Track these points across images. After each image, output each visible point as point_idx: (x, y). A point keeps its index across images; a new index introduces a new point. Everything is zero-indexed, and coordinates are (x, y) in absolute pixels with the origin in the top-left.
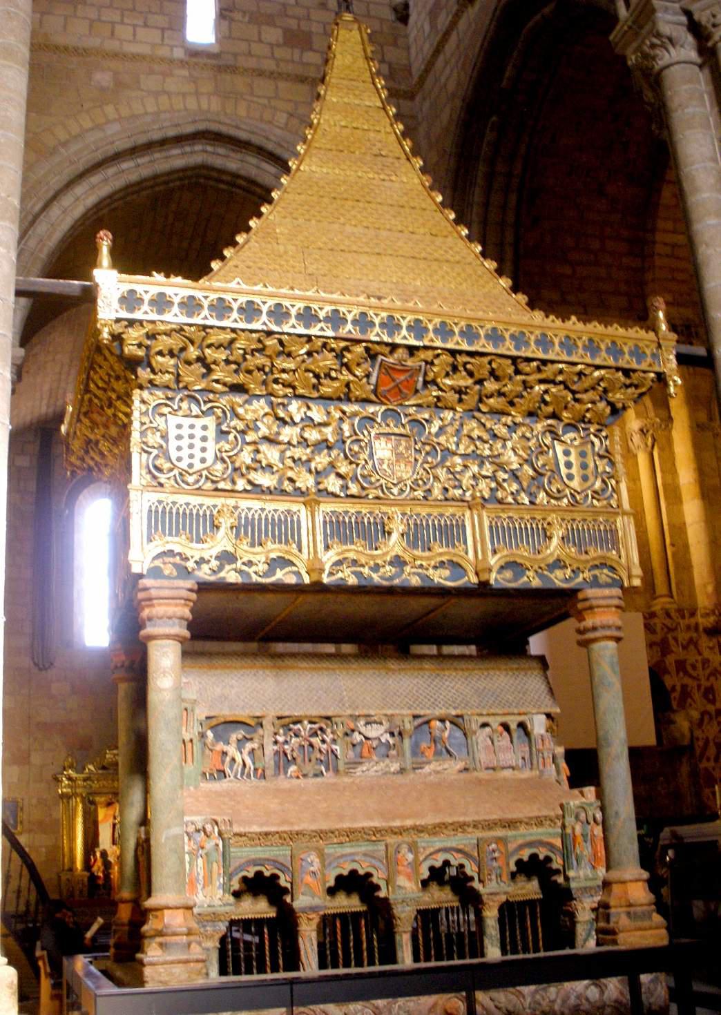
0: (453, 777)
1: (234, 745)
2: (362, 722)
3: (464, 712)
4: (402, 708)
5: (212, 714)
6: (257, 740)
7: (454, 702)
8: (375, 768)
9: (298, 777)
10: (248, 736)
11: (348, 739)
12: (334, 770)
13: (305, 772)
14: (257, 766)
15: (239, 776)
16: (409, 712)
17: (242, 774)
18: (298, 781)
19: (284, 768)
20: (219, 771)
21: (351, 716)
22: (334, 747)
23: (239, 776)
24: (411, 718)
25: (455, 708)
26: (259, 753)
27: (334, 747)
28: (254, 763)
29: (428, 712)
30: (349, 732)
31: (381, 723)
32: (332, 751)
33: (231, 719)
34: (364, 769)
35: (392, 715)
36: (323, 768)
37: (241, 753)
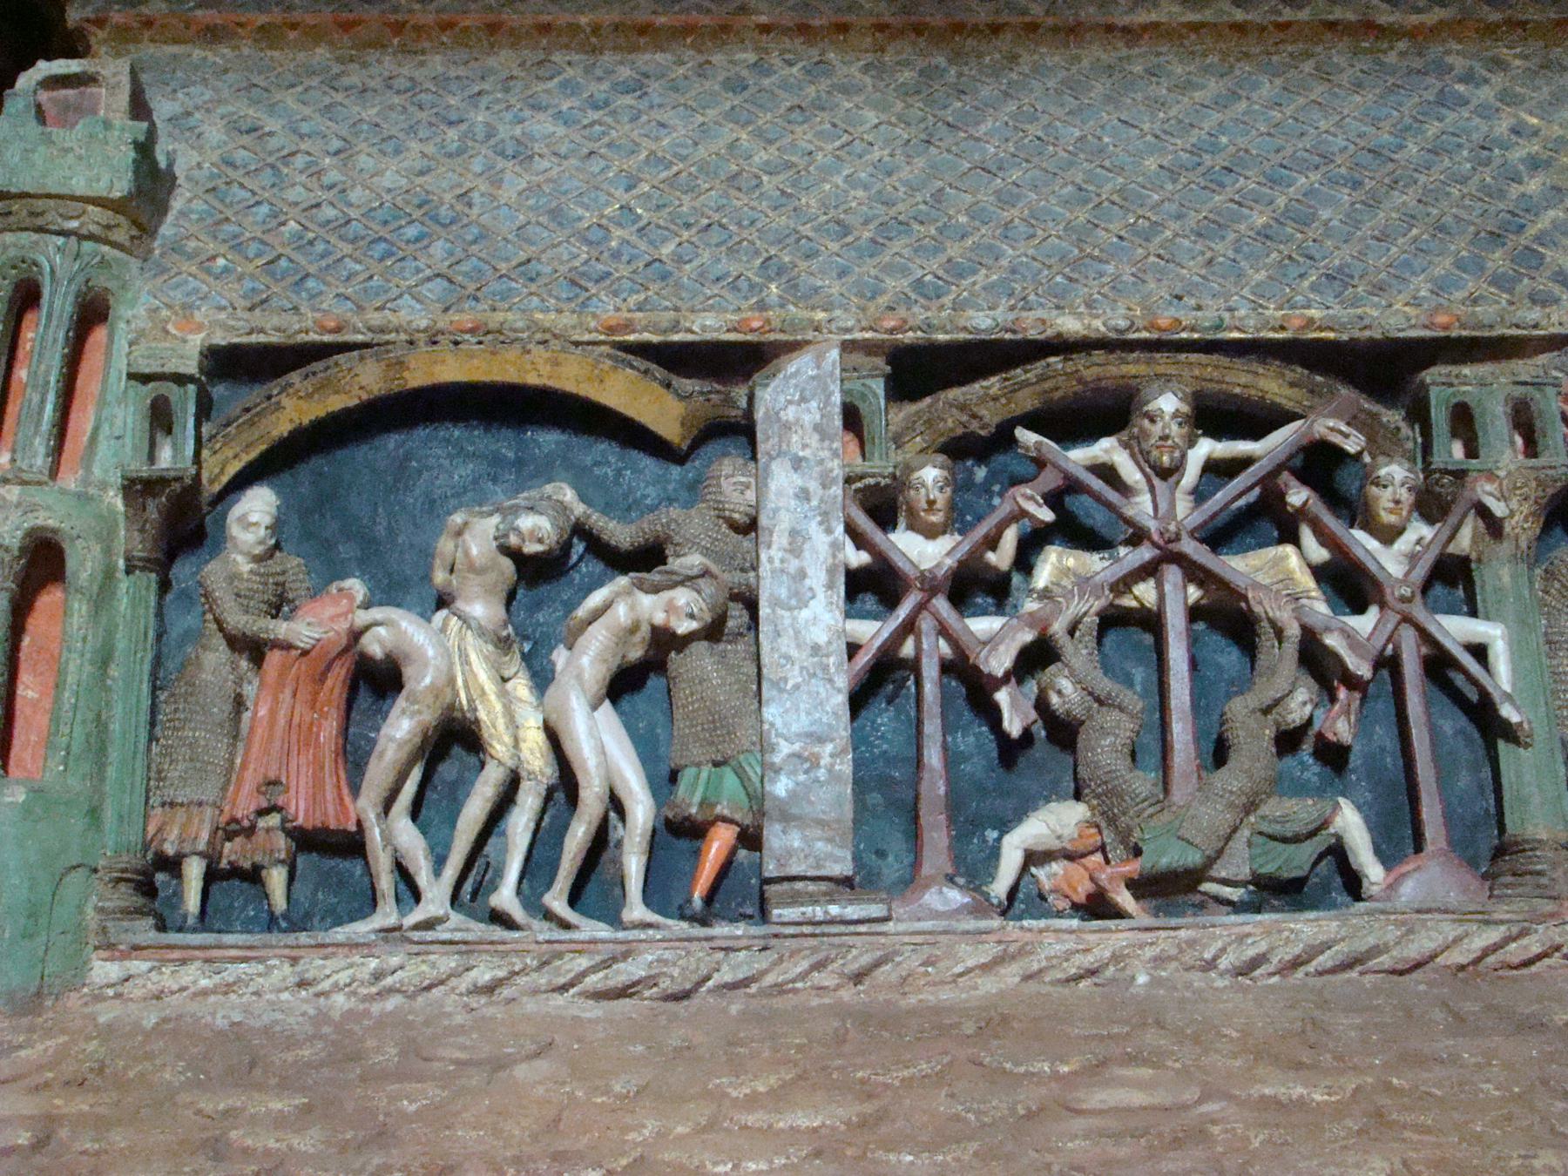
1: (482, 608)
5: (272, 329)
6: (693, 561)
9: (1097, 907)
10: (621, 534)
12: (1462, 846)
13: (1168, 856)
14: (690, 798)
15: (505, 897)
17: (537, 868)
18: (1105, 939)
19: (954, 805)
20: (309, 841)
22: (1455, 629)
23: (505, 897)
26: (698, 664)
27: (1455, 629)
28: (665, 780)
32: (1438, 664)
33: (451, 370)
36: (1351, 823)
37: (542, 679)
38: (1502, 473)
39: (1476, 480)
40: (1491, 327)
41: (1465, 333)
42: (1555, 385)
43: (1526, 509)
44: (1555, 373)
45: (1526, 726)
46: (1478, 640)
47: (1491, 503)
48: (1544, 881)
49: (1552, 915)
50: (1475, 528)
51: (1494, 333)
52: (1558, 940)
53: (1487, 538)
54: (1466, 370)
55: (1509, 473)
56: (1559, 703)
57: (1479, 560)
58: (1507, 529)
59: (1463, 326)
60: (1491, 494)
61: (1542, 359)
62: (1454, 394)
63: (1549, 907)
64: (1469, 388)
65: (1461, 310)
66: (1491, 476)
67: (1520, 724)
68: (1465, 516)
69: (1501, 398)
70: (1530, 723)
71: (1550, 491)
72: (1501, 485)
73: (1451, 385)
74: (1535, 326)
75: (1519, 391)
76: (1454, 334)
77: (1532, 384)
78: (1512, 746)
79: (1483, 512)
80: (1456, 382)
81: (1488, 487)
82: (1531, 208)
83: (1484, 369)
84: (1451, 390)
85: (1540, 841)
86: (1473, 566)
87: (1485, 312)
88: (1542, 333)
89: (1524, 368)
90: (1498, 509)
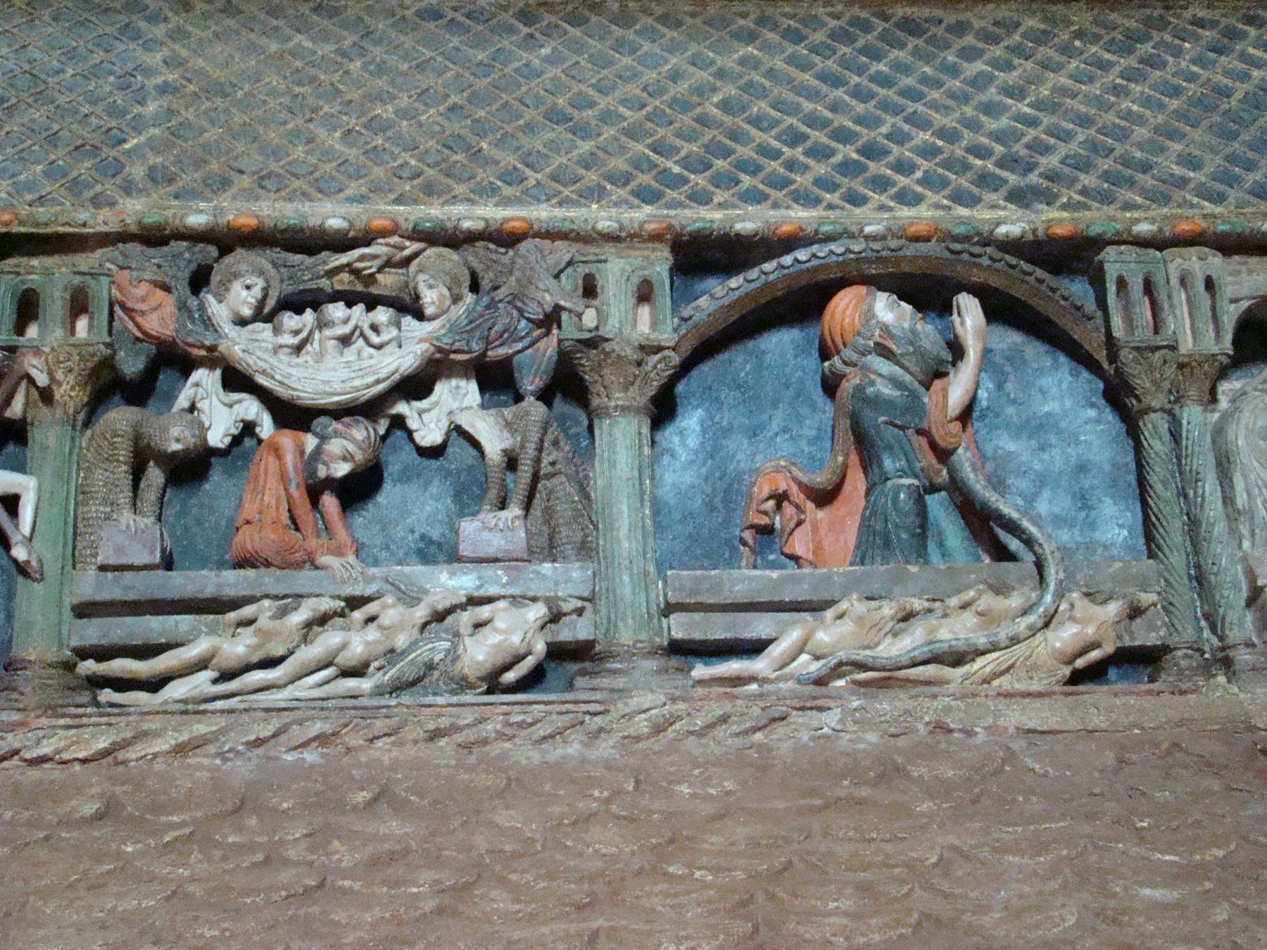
0: (1015, 717)
2: (243, 297)
3: (1097, 220)
4: (595, 194)
7: (1009, 162)
8: (329, 639)
11: (120, 417)
16: (642, 215)
21: (154, 237)
24: (659, 264)
25: (1018, 197)
29: (799, 216)
30: (131, 365)
31: (410, 307)
34: (238, 647)
35: (507, 239)
38: (47, 349)
39: (24, 356)
40: (46, 224)
41: (23, 230)
42: (108, 275)
43: (71, 379)
44: (108, 265)
45: (34, 564)
46: (13, 490)
47: (35, 373)
48: (15, 695)
49: (22, 724)
50: (27, 395)
51: (49, 230)
52: (17, 745)
53: (40, 404)
54: (35, 262)
55: (53, 349)
56: (85, 544)
57: (32, 424)
58: (57, 396)
59: (21, 223)
60: (34, 366)
61: (99, 253)
62: (23, 282)
63: (16, 717)
64: (35, 277)
65: (24, 211)
66: (37, 351)
67: (28, 562)
68: (17, 385)
69: (60, 286)
70: (40, 561)
71: (90, 365)
72: (47, 359)
73: (18, 274)
74: (84, 225)
75: (77, 280)
76: (16, 229)
77: (90, 274)
78: (29, 581)
79: (32, 381)
80: (22, 271)
81: (34, 362)
82: (138, 125)
83: (49, 261)
84: (20, 278)
85: (30, 661)
86: (29, 428)
87: (42, 212)
88: (91, 230)
89: (86, 261)
90: (42, 380)
